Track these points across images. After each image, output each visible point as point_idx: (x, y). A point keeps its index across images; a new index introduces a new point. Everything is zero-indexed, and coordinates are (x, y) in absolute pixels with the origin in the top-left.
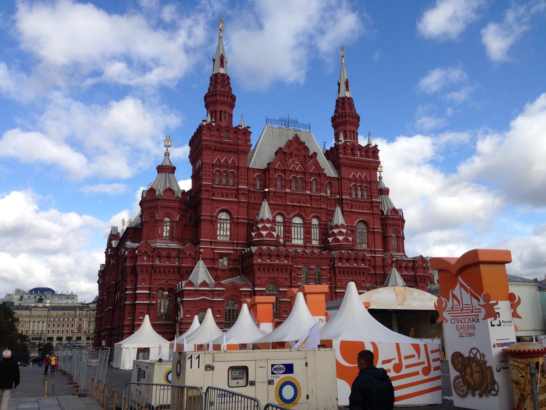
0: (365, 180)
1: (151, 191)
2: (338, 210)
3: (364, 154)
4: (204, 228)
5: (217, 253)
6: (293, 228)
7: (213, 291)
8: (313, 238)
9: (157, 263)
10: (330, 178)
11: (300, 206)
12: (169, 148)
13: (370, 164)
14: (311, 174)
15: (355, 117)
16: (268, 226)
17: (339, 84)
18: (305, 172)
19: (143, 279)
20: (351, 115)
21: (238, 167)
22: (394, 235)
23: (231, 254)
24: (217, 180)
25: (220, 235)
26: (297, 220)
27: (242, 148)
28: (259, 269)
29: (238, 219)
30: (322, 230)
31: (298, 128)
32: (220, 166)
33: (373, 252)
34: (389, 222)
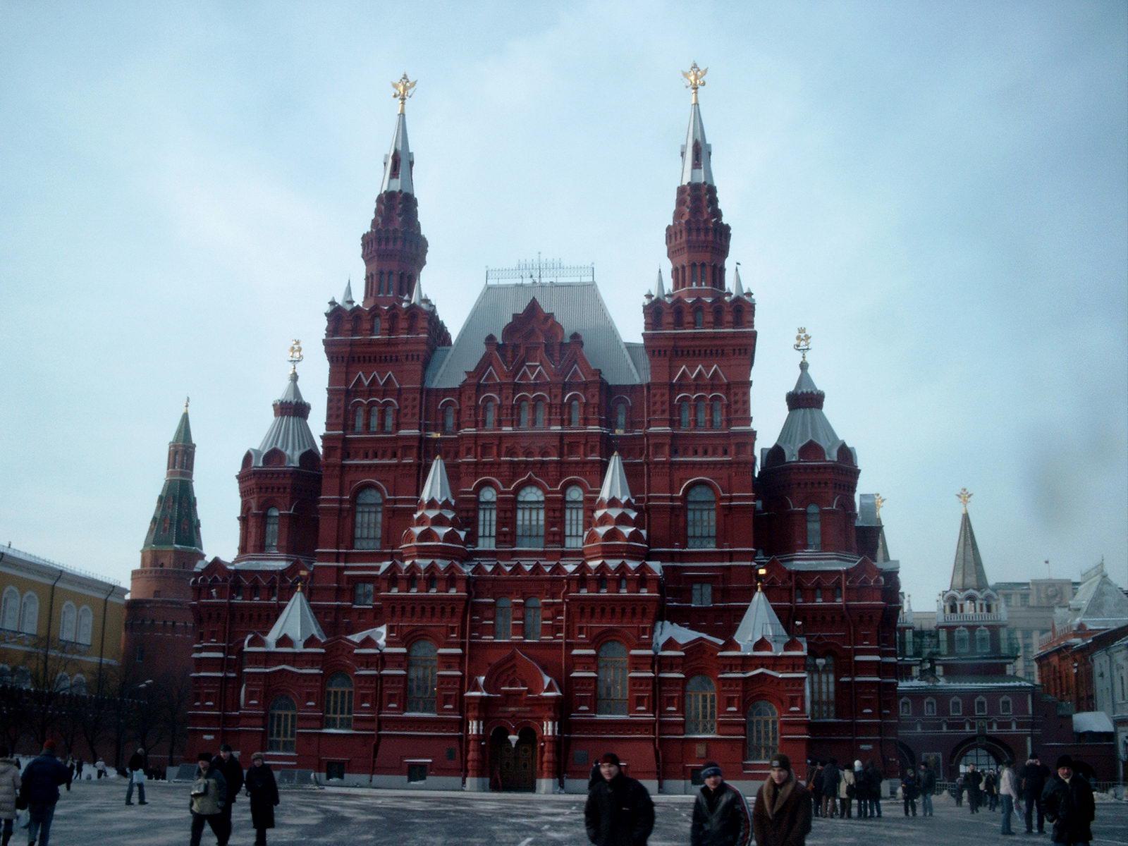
0: (716, 382)
1: (248, 458)
2: (615, 464)
3: (710, 318)
4: (327, 527)
5: (349, 577)
6: (520, 514)
7: (301, 654)
8: (568, 533)
9: (238, 600)
10: (625, 387)
11: (534, 463)
12: (298, 365)
13: (726, 342)
14: (566, 387)
15: (707, 230)
16: (431, 514)
17: (682, 154)
18: (548, 383)
19: (213, 632)
20: (693, 226)
21: (400, 390)
22: (813, 509)
23: (376, 577)
24: (360, 422)
25: (362, 538)
26: (532, 495)
27: (408, 347)
28: (393, 607)
29: (395, 501)
30: (590, 514)
31: (561, 280)
32: (361, 394)
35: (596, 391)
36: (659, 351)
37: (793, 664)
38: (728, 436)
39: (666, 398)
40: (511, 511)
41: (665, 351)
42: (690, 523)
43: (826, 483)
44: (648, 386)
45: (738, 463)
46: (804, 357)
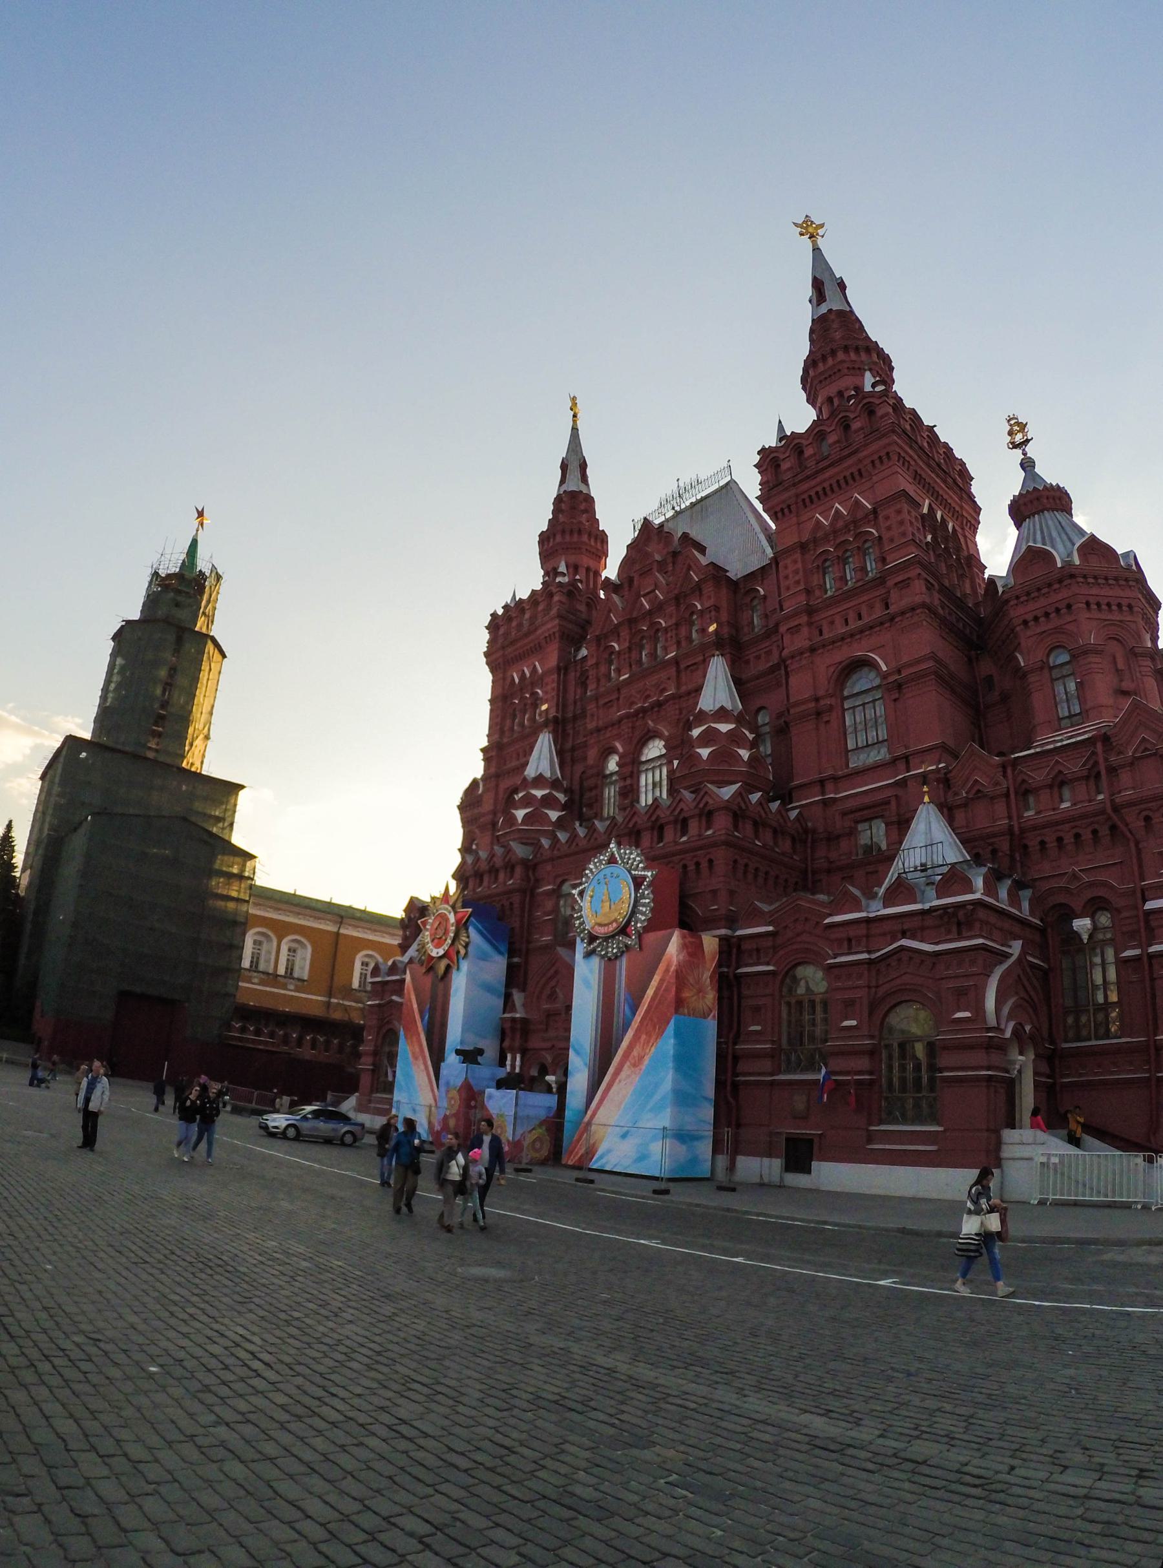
0: (860, 515)
11: (652, 707)
26: (655, 749)
31: (703, 494)
33: (901, 765)
34: (1017, 613)
35: (708, 589)
36: (782, 510)
37: (955, 920)
38: (880, 580)
39: (799, 565)
40: (631, 776)
41: (789, 506)
42: (850, 730)
43: (1069, 607)
44: (775, 560)
45: (903, 613)
46: (1025, 454)
